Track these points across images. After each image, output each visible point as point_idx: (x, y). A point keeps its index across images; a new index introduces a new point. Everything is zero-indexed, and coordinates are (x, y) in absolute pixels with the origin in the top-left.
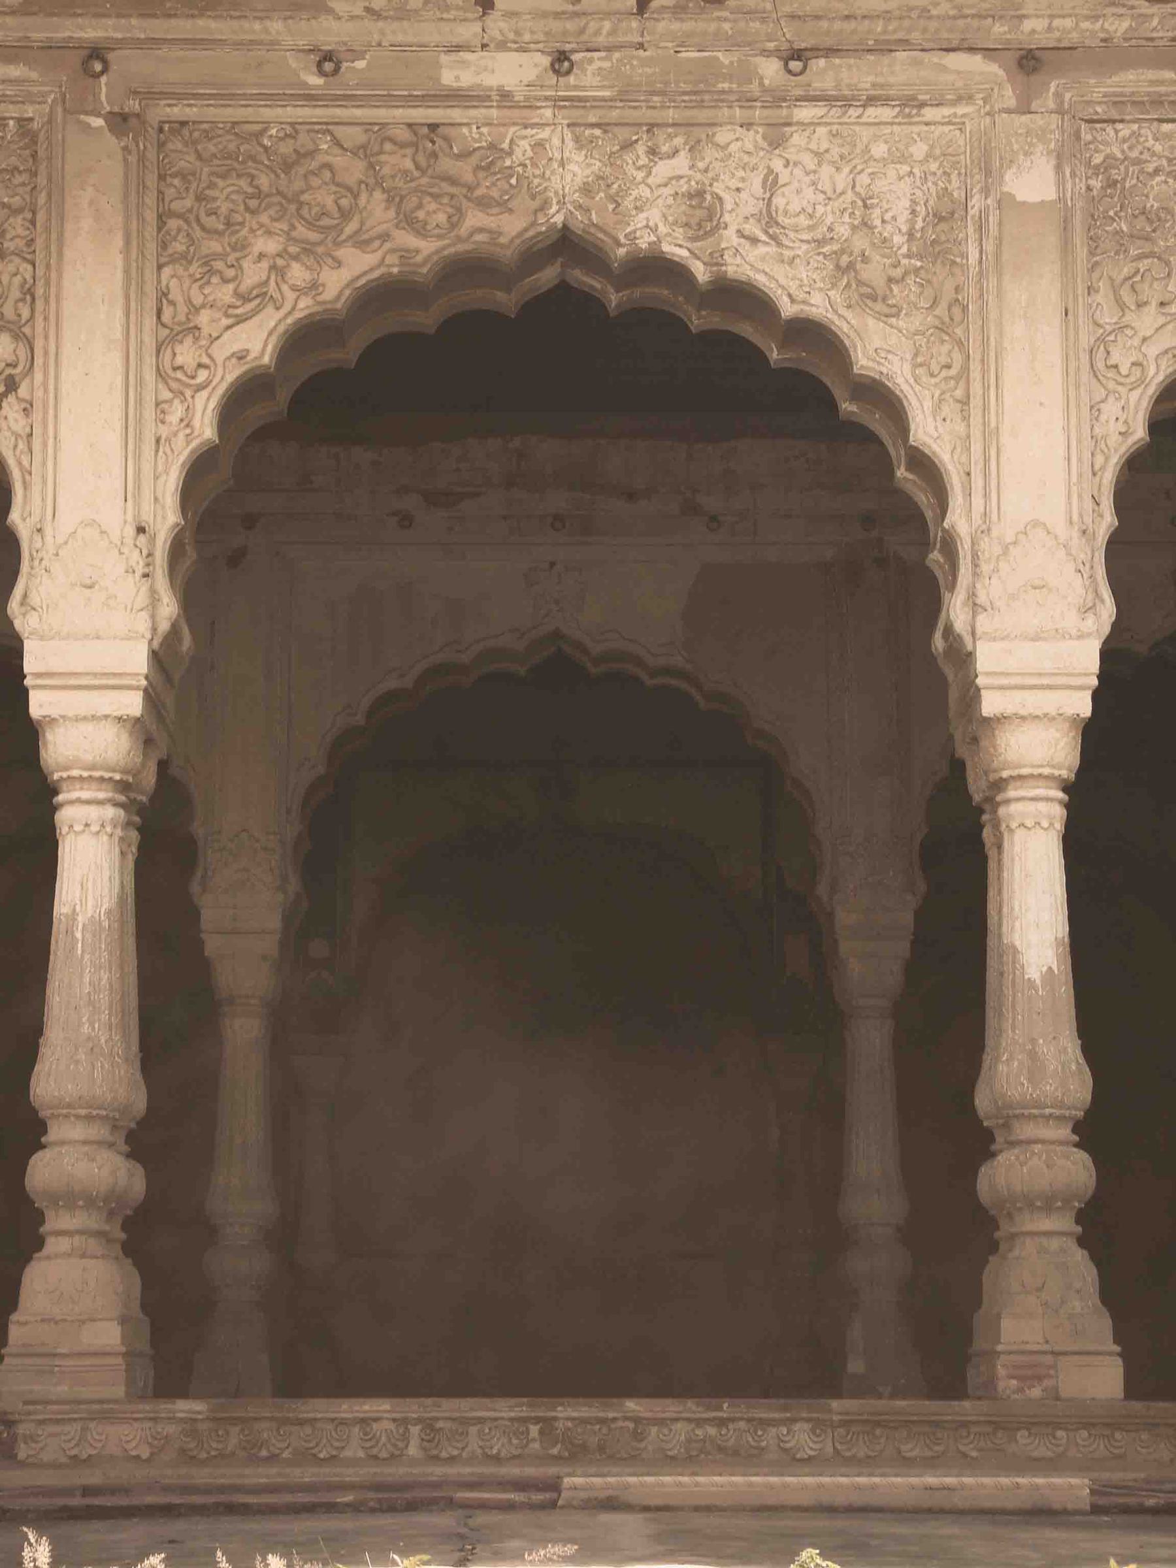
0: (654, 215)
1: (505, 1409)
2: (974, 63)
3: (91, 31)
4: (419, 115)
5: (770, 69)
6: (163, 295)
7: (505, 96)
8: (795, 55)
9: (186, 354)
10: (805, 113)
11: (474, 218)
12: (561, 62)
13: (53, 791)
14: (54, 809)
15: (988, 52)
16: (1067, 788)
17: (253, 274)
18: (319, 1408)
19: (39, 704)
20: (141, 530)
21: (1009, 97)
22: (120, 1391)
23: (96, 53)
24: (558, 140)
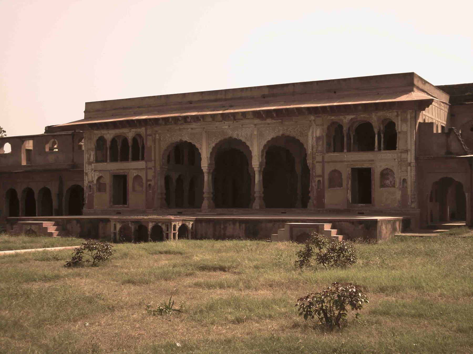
0: (235, 136)
1: (226, 209)
2: (252, 125)
3: (204, 126)
4: (222, 130)
5: (241, 126)
6: (208, 142)
7: (226, 129)
8: (243, 125)
9: (210, 146)
10: (243, 128)
11: (225, 136)
12: (229, 126)
13: (204, 173)
14: (204, 174)
15: (253, 124)
16: (259, 171)
17: (213, 141)
18: (217, 209)
19: (202, 168)
20: (207, 157)
21: (254, 127)
22: (207, 208)
23: (204, 128)
24: (230, 131)
